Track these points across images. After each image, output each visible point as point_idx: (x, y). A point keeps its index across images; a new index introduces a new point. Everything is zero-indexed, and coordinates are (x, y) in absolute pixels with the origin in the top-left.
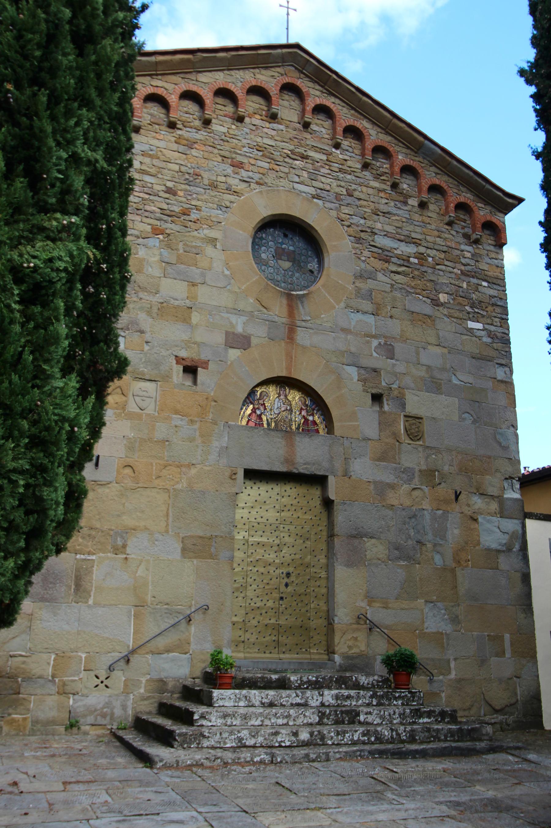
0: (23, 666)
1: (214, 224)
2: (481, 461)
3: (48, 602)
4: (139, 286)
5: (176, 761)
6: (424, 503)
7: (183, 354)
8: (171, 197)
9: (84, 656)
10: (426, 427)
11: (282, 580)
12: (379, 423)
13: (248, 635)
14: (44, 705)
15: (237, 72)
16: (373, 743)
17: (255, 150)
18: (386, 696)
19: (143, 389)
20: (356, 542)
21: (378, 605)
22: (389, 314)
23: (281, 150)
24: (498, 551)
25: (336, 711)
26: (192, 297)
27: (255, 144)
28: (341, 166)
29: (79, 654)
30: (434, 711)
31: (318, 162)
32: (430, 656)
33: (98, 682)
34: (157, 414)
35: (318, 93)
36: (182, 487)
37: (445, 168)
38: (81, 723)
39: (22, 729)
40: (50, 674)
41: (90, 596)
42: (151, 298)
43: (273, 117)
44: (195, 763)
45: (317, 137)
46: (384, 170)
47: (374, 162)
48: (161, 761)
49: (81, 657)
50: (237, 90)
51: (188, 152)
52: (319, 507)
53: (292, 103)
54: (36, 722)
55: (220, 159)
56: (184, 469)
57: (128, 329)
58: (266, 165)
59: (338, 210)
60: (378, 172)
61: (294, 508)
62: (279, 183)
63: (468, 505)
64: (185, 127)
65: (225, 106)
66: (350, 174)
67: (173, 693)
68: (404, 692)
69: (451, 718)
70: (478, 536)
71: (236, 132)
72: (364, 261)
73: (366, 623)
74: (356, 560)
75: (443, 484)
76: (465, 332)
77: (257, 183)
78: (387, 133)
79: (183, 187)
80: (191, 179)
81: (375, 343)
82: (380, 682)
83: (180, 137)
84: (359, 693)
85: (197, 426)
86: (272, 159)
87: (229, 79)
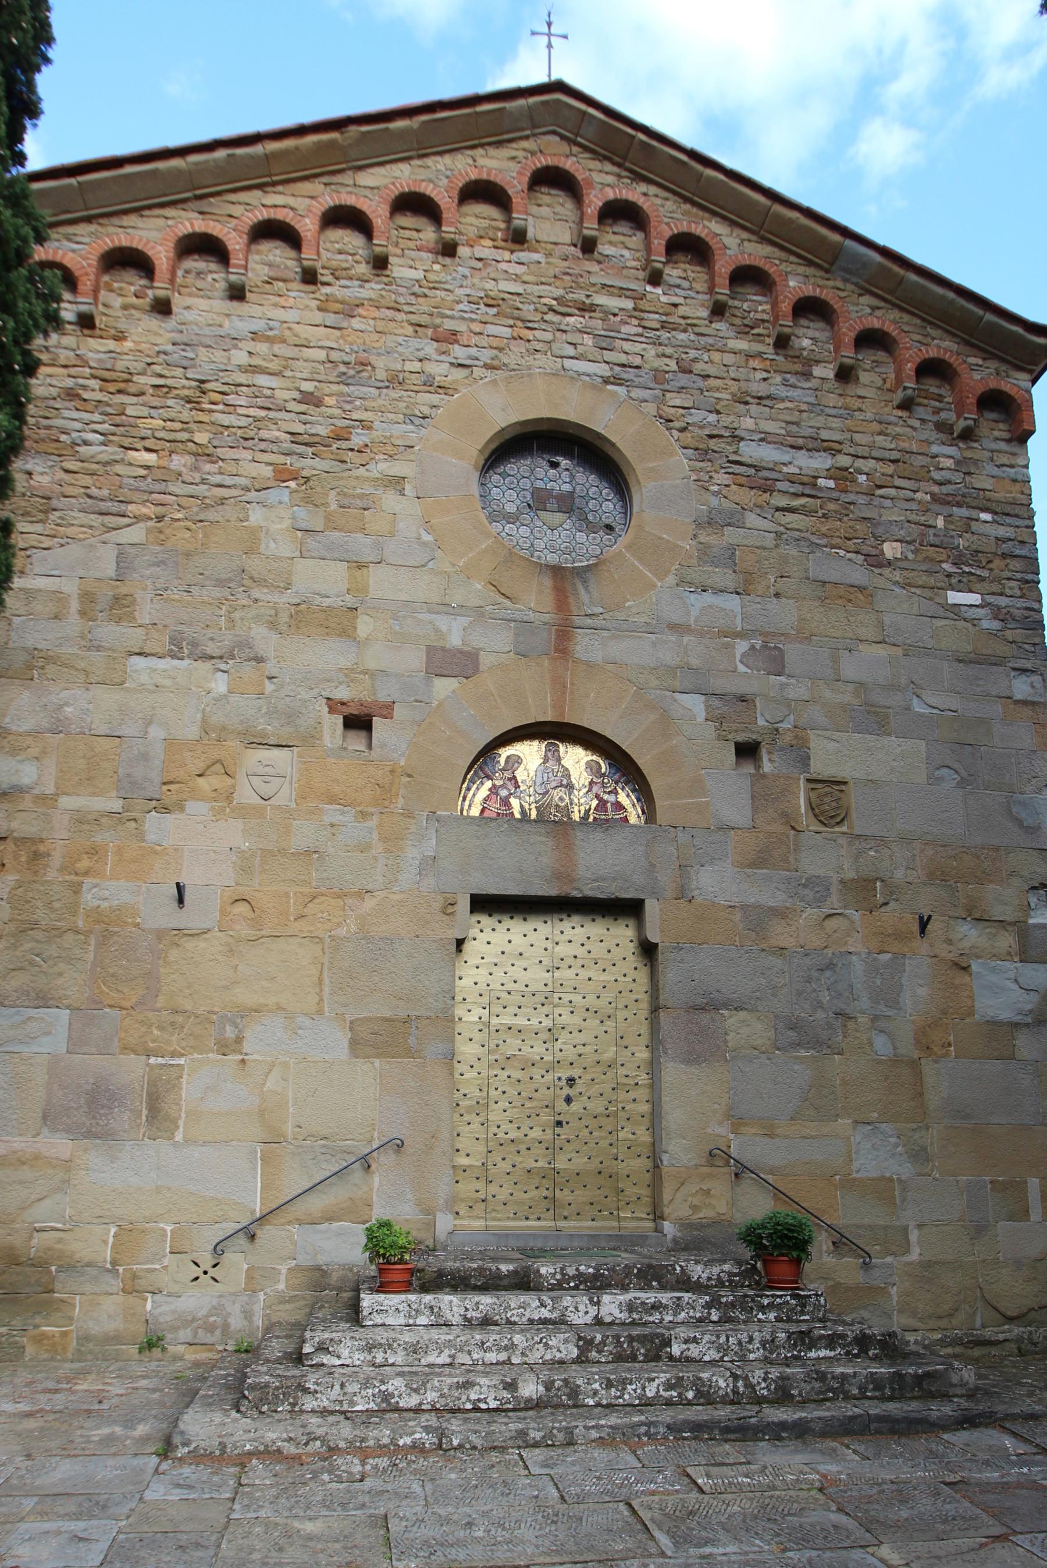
0: (59, 1246)
1: (395, 451)
2: (978, 858)
3: (100, 1138)
4: (252, 578)
5: (220, 1443)
6: (851, 941)
7: (342, 693)
8: (311, 409)
9: (169, 1228)
10: (854, 798)
11: (558, 1091)
12: (753, 797)
13: (493, 1189)
14: (98, 1310)
15: (438, 158)
16: (689, 1403)
17: (482, 306)
18: (741, 1303)
19: (264, 763)
20: (705, 1018)
21: (753, 1131)
22: (772, 591)
23: (535, 300)
24: (1017, 1025)
25: (617, 1337)
26: (358, 589)
27: (482, 295)
28: (664, 318)
29: (161, 1225)
30: (843, 1336)
31: (615, 315)
32: (866, 1221)
33: (198, 1272)
34: (293, 805)
35: (610, 179)
36: (349, 931)
37: (891, 292)
38: (168, 1340)
39: (60, 1351)
40: (109, 1259)
41: (178, 1127)
42: (276, 598)
43: (518, 238)
44: (262, 1448)
45: (612, 267)
46: (759, 316)
47: (736, 303)
48: (185, 1444)
49: (165, 1231)
50: (440, 192)
51: (345, 324)
52: (631, 958)
53: (558, 209)
54: (85, 1338)
55: (410, 330)
56: (349, 901)
57: (233, 657)
58: (507, 332)
59: (661, 401)
60: (746, 322)
61: (580, 962)
62: (532, 362)
63: (949, 942)
64: (337, 279)
65: (418, 231)
66: (685, 331)
67: (340, 1290)
68: (781, 1297)
69: (882, 1349)
70: (971, 998)
71: (442, 277)
72: (716, 494)
73: (728, 1164)
74: (704, 1050)
75: (892, 904)
76: (941, 612)
77: (486, 366)
78: (764, 240)
79: (335, 388)
80: (352, 372)
81: (742, 646)
82: (735, 1275)
83: (328, 298)
84: (679, 1298)
85: (373, 822)
86: (518, 319)
87: (423, 174)
